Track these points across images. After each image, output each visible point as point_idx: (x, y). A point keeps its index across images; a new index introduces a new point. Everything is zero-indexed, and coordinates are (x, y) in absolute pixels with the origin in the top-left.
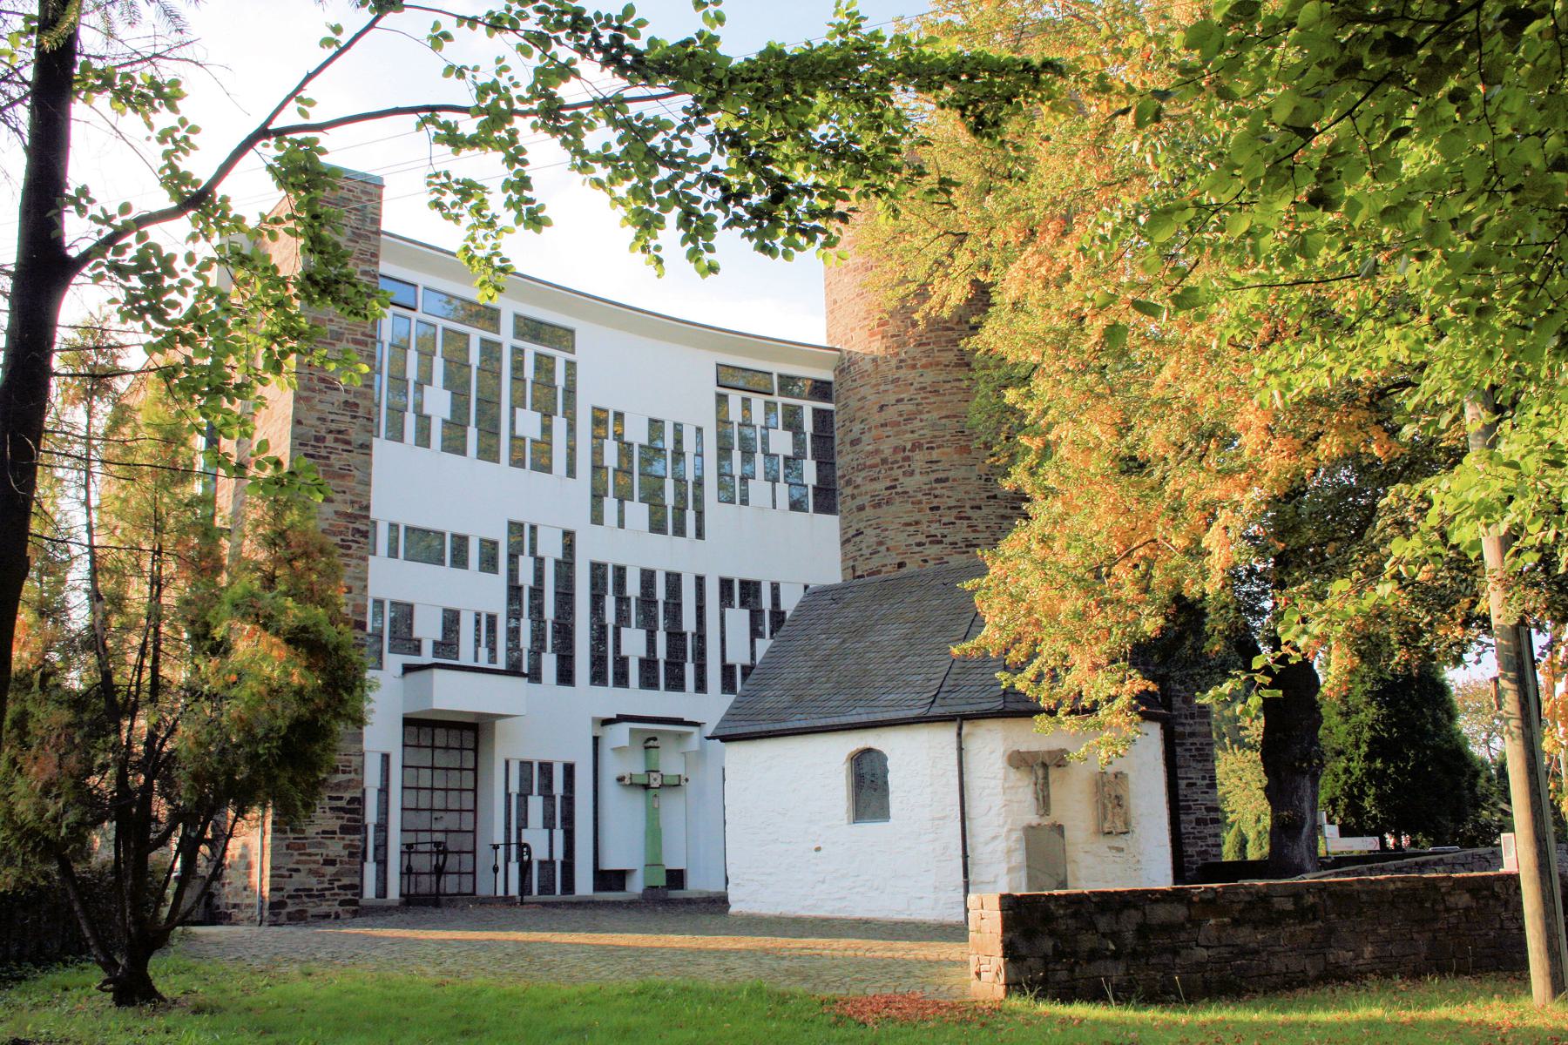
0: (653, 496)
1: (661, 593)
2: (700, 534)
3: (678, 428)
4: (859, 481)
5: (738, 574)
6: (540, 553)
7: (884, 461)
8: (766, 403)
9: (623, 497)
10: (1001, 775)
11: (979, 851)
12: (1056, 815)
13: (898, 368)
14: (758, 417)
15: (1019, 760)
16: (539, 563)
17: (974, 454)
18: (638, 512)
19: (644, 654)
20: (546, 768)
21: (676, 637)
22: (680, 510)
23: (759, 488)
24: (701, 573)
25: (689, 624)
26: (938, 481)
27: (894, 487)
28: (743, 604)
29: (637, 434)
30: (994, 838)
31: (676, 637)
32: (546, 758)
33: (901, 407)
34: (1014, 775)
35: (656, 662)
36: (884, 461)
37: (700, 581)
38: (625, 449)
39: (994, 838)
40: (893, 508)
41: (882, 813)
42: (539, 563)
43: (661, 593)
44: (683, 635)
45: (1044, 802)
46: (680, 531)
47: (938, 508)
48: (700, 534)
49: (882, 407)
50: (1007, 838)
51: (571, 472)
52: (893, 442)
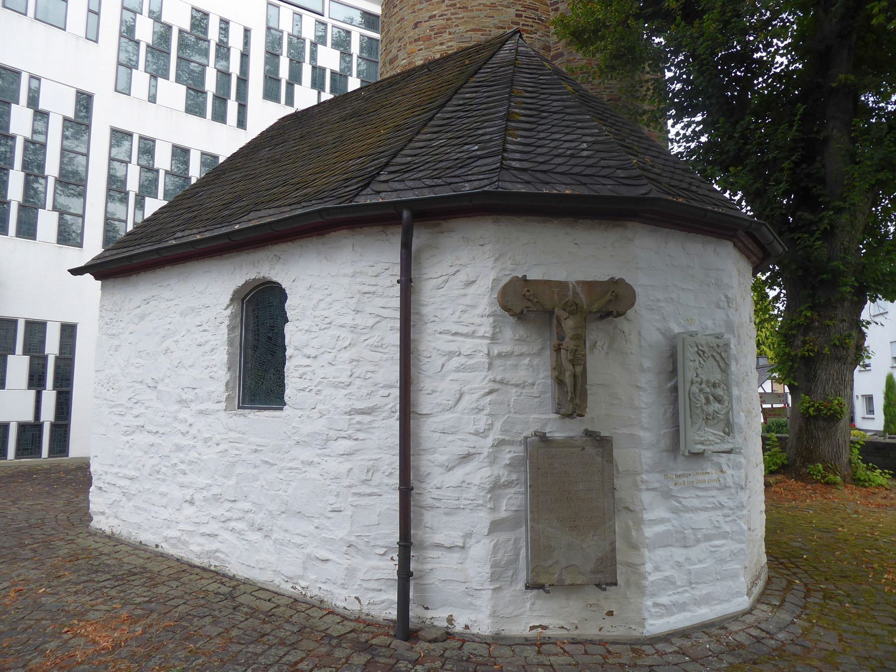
3: (225, 24)
6: (42, 106)
9: (158, 73)
10: (486, 328)
11: (438, 482)
12: (599, 413)
15: (525, 303)
18: (173, 92)
20: (36, 329)
22: (221, 100)
29: (179, 19)
30: (466, 458)
32: (36, 315)
33: (432, 23)
34: (510, 333)
39: (466, 458)
46: (220, 116)
49: (416, 25)
50: (493, 460)
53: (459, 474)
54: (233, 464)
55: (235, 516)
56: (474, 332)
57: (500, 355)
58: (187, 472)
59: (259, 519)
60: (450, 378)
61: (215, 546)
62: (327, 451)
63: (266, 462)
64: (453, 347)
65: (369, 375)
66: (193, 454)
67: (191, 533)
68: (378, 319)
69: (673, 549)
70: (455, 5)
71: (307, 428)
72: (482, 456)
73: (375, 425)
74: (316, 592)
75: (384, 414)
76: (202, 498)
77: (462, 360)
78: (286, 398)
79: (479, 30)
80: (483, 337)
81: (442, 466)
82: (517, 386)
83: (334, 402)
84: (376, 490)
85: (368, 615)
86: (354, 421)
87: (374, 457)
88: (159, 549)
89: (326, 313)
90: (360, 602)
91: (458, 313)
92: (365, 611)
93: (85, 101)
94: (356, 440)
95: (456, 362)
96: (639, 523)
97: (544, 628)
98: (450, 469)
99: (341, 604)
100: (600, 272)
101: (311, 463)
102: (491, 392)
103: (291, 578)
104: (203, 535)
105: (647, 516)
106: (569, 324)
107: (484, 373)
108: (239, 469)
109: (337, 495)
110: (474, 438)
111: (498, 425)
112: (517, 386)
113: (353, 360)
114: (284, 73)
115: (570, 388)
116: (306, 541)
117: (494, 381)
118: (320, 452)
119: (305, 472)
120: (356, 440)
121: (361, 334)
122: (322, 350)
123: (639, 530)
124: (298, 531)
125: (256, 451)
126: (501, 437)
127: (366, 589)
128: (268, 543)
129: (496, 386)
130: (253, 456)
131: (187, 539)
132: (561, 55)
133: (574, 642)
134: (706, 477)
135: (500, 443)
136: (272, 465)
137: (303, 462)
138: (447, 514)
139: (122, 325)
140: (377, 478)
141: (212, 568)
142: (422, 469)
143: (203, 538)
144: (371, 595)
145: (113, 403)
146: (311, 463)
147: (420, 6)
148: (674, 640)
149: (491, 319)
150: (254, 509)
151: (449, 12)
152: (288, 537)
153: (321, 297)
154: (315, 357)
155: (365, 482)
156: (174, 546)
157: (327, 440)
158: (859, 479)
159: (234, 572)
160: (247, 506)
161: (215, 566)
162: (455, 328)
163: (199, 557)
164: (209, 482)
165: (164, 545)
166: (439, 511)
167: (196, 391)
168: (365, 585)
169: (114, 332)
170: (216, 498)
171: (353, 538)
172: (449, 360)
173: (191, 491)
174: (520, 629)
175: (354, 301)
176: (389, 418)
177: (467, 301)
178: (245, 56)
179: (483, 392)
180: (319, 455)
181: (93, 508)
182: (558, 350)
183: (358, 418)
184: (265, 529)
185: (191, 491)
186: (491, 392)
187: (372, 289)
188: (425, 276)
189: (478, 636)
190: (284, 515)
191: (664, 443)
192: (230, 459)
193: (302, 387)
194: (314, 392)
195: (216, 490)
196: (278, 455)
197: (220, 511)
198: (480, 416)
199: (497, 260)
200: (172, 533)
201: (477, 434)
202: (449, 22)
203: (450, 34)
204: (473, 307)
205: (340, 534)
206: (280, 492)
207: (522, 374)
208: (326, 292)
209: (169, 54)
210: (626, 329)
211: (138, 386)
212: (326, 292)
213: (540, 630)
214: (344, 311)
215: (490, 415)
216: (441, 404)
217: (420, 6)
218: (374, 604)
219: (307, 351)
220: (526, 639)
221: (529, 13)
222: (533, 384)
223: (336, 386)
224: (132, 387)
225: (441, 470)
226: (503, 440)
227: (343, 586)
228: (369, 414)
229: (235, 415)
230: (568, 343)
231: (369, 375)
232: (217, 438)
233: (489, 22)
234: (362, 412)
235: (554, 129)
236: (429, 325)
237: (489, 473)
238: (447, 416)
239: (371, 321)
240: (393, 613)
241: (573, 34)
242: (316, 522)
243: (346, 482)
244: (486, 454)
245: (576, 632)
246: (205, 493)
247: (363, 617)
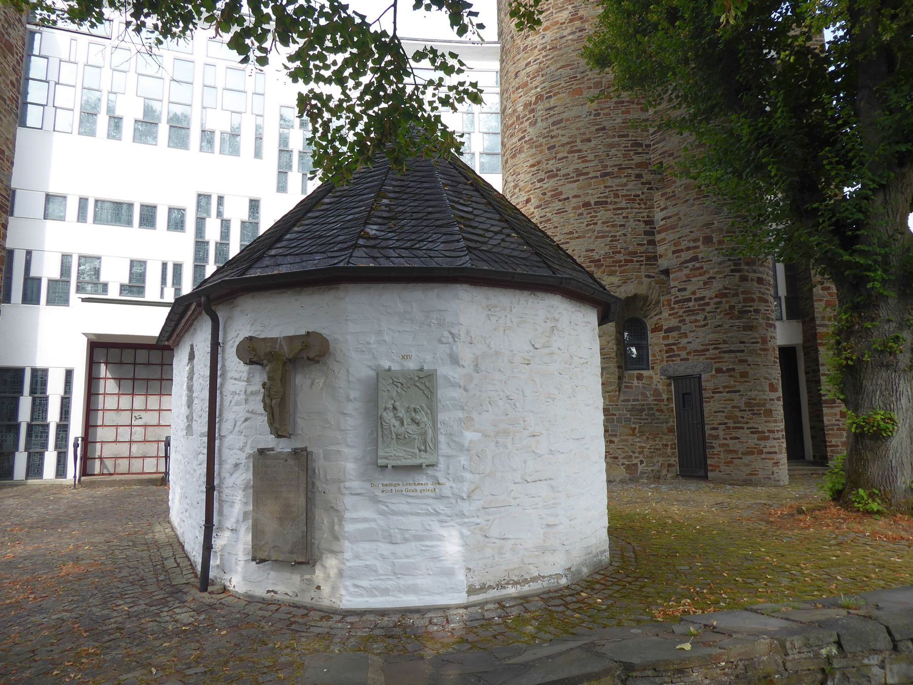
16: (226, 226)
26: (554, 124)
33: (528, 69)
36: (518, 118)
40: (523, 155)
42: (226, 226)
47: (554, 147)
51: (258, 154)
52: (524, 100)
57: (252, 393)
69: (379, 544)
70: (545, 47)
79: (568, 65)
93: (254, 205)
96: (341, 519)
97: (276, 593)
102: (246, 420)
105: (347, 515)
123: (341, 525)
129: (249, 415)
151: (541, 56)
174: (259, 592)
199: (252, 324)
220: (263, 599)
245: (296, 599)
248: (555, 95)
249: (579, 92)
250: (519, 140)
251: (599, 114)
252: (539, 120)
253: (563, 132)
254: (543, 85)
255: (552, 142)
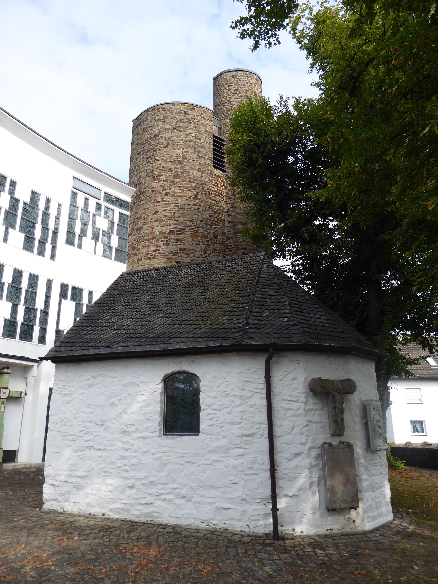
0: (28, 227)
1: (25, 284)
2: (53, 257)
3: (48, 201)
4: (140, 247)
5: (72, 283)
7: (154, 238)
8: (97, 203)
10: (303, 398)
13: (165, 195)
14: (92, 208)
17: (199, 239)
18: (17, 237)
19: (8, 317)
21: (30, 310)
22: (42, 243)
23: (88, 241)
24: (50, 278)
25: (39, 304)
26: (180, 249)
27: (159, 250)
28: (73, 299)
29: (23, 196)
30: (298, 455)
31: (30, 310)
33: (165, 213)
35: (16, 323)
37: (49, 283)
38: (14, 202)
39: (298, 455)
40: (157, 260)
41: (192, 428)
43: (25, 284)
44: (35, 310)
45: (338, 426)
46: (41, 253)
48: (53, 257)
49: (155, 213)
50: (309, 455)
52: (160, 229)
53: (295, 462)
54: (165, 464)
55: (167, 492)
56: (298, 400)
58: (129, 470)
59: (183, 492)
60: (288, 420)
61: (150, 509)
62: (228, 455)
63: (189, 462)
64: (288, 406)
65: (250, 418)
66: (134, 461)
67: (132, 504)
68: (253, 393)
69: (371, 492)
70: (178, 206)
71: (215, 444)
72: (304, 454)
73: (254, 441)
74: (221, 526)
75: (258, 436)
76: (141, 484)
77: (293, 412)
78: (201, 429)
80: (302, 402)
81: (287, 459)
82: (315, 423)
83: (231, 431)
84: (256, 472)
85: (253, 533)
86: (243, 440)
87: (254, 456)
88: (106, 516)
89: (225, 390)
90: (249, 527)
91: (290, 392)
92: (252, 531)
94: (245, 448)
95: (290, 413)
96: (361, 480)
97: (332, 530)
98: (290, 460)
99: (238, 529)
100: (344, 376)
101: (218, 461)
102: (306, 426)
103: (206, 520)
104: (141, 504)
106: (338, 397)
107: (303, 418)
108: (170, 467)
109: (235, 476)
110: (300, 446)
111: (310, 440)
112: (315, 423)
113: (242, 412)
114: (78, 230)
115: (340, 424)
116: (215, 500)
117: (307, 421)
118: (223, 455)
119: (215, 465)
120: (245, 448)
121: (245, 400)
122: (223, 407)
124: (210, 496)
125: (182, 457)
126: (312, 445)
127: (252, 520)
128: (189, 504)
129: (308, 423)
130: (179, 459)
131: (129, 508)
132: (232, 238)
133: (343, 535)
134: (377, 461)
135: (312, 448)
136: (193, 463)
137: (213, 461)
138: (290, 481)
139: (73, 389)
140: (256, 466)
141: (149, 522)
142: (278, 461)
143: (142, 506)
144: (254, 523)
145: (66, 434)
146: (218, 461)
147: (159, 204)
148: (381, 530)
149: (304, 395)
150: (180, 487)
151: (175, 210)
152: (204, 499)
153: (222, 382)
154: (220, 410)
155: (250, 468)
156: (119, 513)
157: (229, 449)
158: (394, 466)
159: (167, 522)
160: (175, 486)
161: (151, 521)
162: (289, 398)
163: (138, 517)
164: (147, 475)
165: (110, 513)
166: (285, 479)
167: (136, 426)
168: (252, 518)
169: (66, 393)
170: (152, 483)
171: (244, 496)
172: (286, 412)
173: (133, 481)
174: (323, 531)
175: (240, 385)
176: (260, 438)
177: (293, 386)
178: (57, 218)
179: (303, 426)
180: (223, 457)
181: (45, 496)
182: (334, 408)
183: (245, 438)
184: (187, 497)
185: (133, 481)
186: (306, 426)
187: (250, 380)
188: (274, 375)
189: (307, 535)
190: (201, 489)
191: (365, 446)
192: (163, 462)
193: (212, 424)
194: (219, 427)
195: (152, 479)
196: (197, 458)
197: (153, 490)
198: (303, 436)
199: (305, 370)
200: (118, 505)
201: (301, 444)
202: (175, 215)
203: (175, 220)
204: (296, 389)
205: (238, 494)
206: (199, 477)
207: (316, 418)
208: (225, 380)
209: (16, 215)
210: (350, 399)
211: (87, 424)
212: (225, 380)
213: (330, 531)
214: (236, 389)
215: (307, 435)
216: (285, 431)
217: (159, 204)
218: (256, 527)
219: (215, 407)
220: (326, 535)
221: (215, 215)
222: (321, 422)
223: (232, 423)
224: (83, 424)
225: (286, 461)
226: (312, 446)
227: (240, 520)
228: (251, 436)
229: (166, 438)
230: (337, 405)
231: (250, 418)
232: (153, 451)
233: (196, 217)
234: (247, 436)
235: (310, 312)
236: (277, 396)
237: (308, 461)
238: (288, 436)
239: (250, 394)
240: (271, 529)
241: (252, 237)
242: (222, 490)
243: (241, 469)
244: (306, 453)
245: (343, 531)
246: (144, 481)
247: (251, 534)
248: (182, 234)
249: (196, 237)
250: (154, 251)
251: (205, 253)
252: (171, 244)
253: (186, 256)
254: (175, 226)
255: (179, 259)
